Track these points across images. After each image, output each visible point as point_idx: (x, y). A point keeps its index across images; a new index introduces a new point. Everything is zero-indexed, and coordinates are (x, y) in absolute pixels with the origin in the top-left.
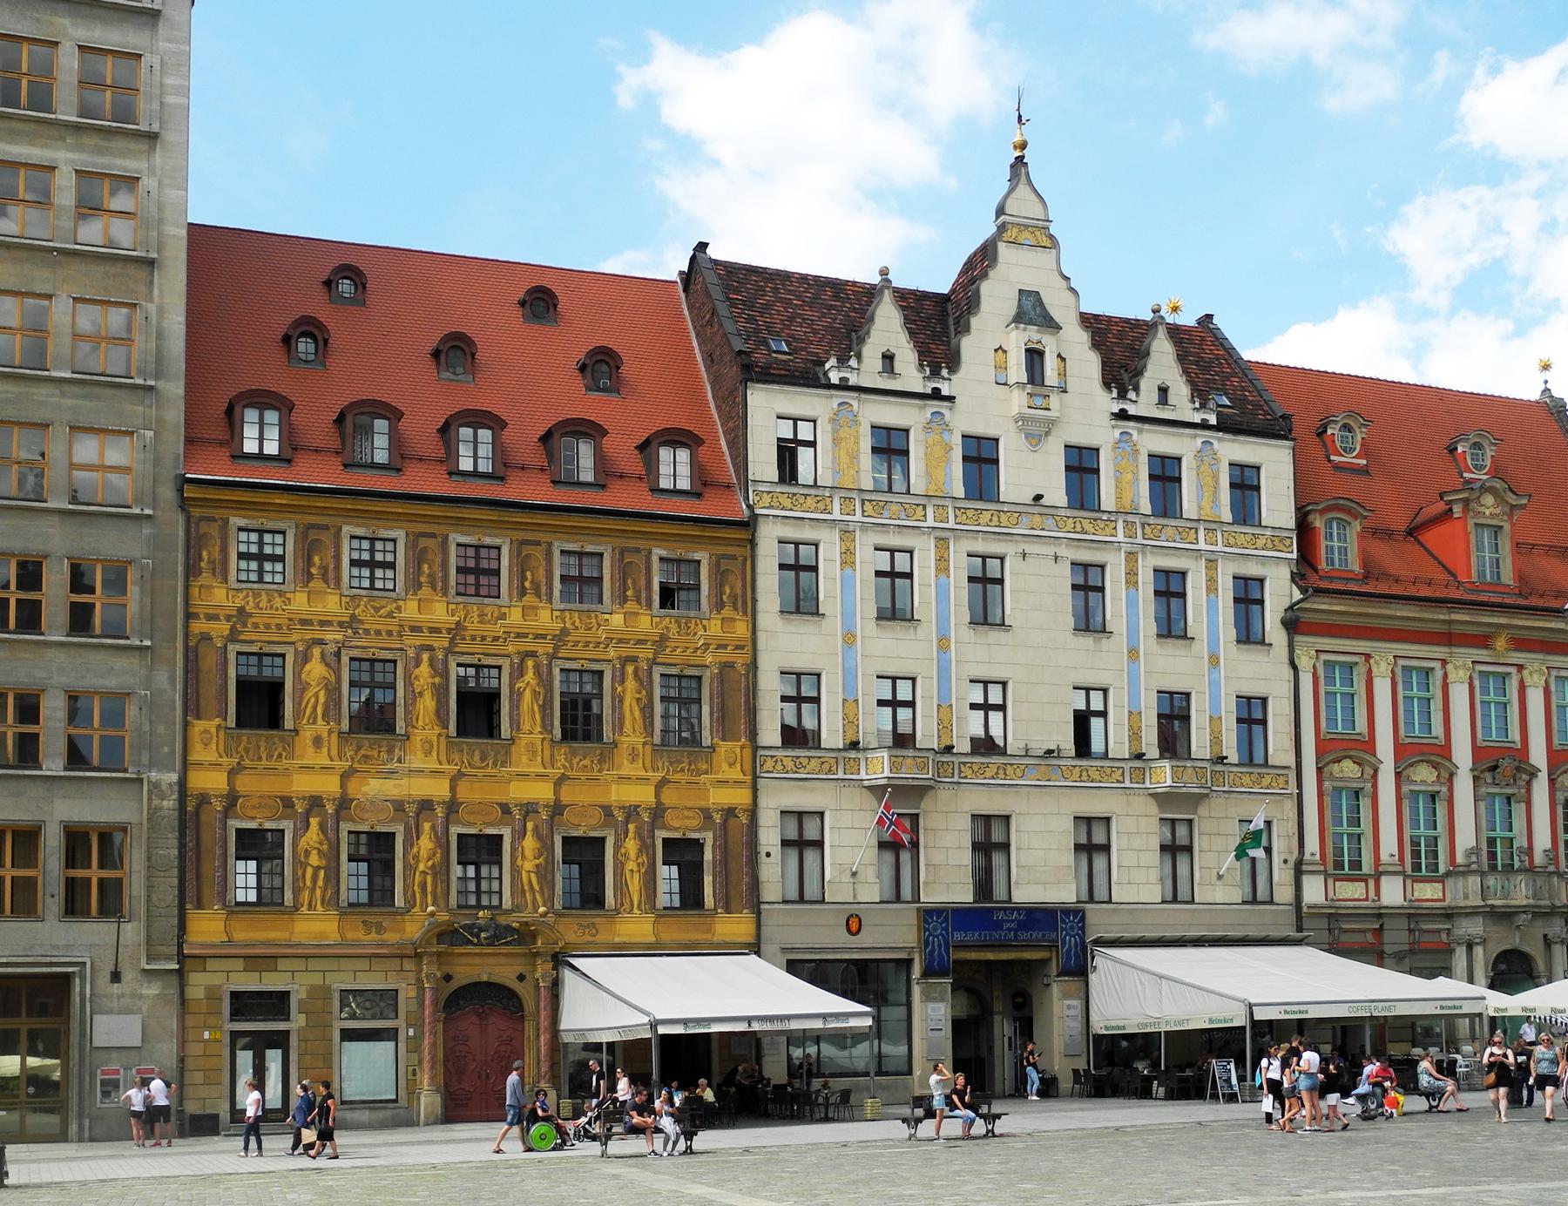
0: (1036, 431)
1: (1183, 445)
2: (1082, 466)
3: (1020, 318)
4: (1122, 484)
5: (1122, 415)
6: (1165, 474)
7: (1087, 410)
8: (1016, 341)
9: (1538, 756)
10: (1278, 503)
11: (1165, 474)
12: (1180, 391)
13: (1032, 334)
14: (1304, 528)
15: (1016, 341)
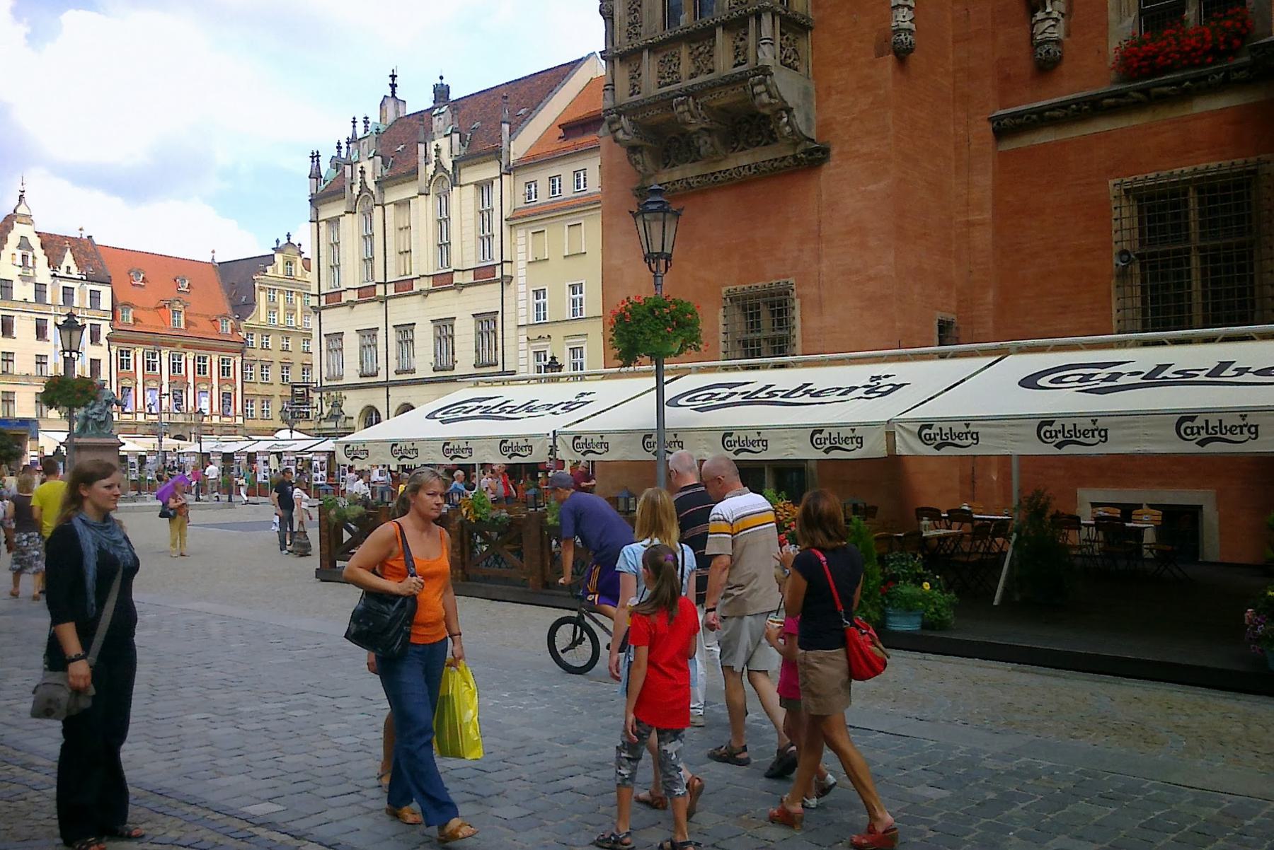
0: (25, 279)
1: (76, 285)
2: (40, 289)
3: (20, 247)
4: (54, 294)
5: (54, 275)
6: (68, 293)
7: (43, 273)
8: (19, 253)
9: (191, 380)
10: (106, 303)
11: (68, 293)
12: (74, 270)
13: (25, 252)
14: (114, 310)
15: (19, 253)
